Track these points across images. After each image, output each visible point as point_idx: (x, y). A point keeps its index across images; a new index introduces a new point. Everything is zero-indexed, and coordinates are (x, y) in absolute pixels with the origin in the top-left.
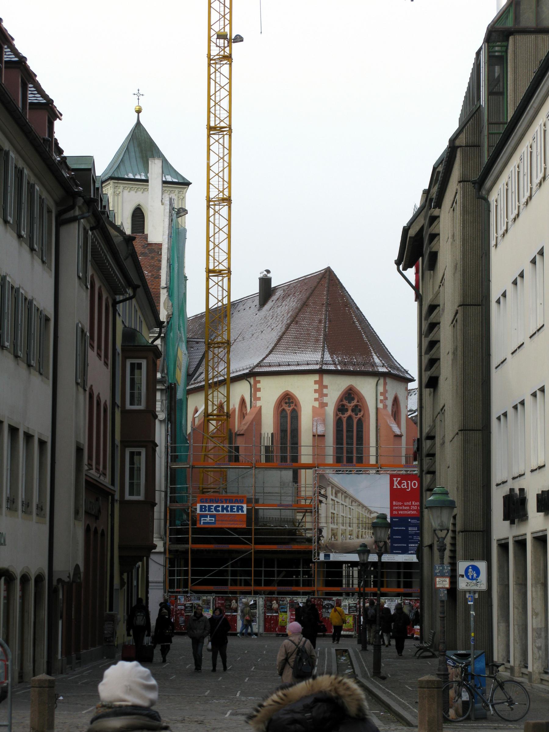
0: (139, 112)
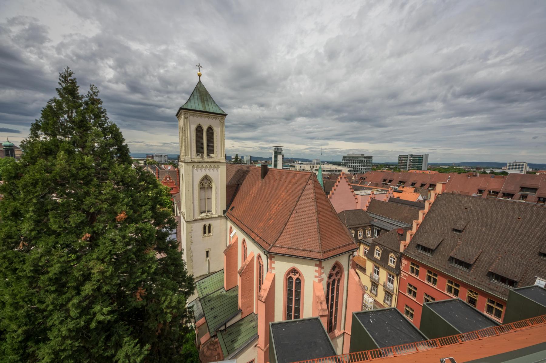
0: (200, 75)
